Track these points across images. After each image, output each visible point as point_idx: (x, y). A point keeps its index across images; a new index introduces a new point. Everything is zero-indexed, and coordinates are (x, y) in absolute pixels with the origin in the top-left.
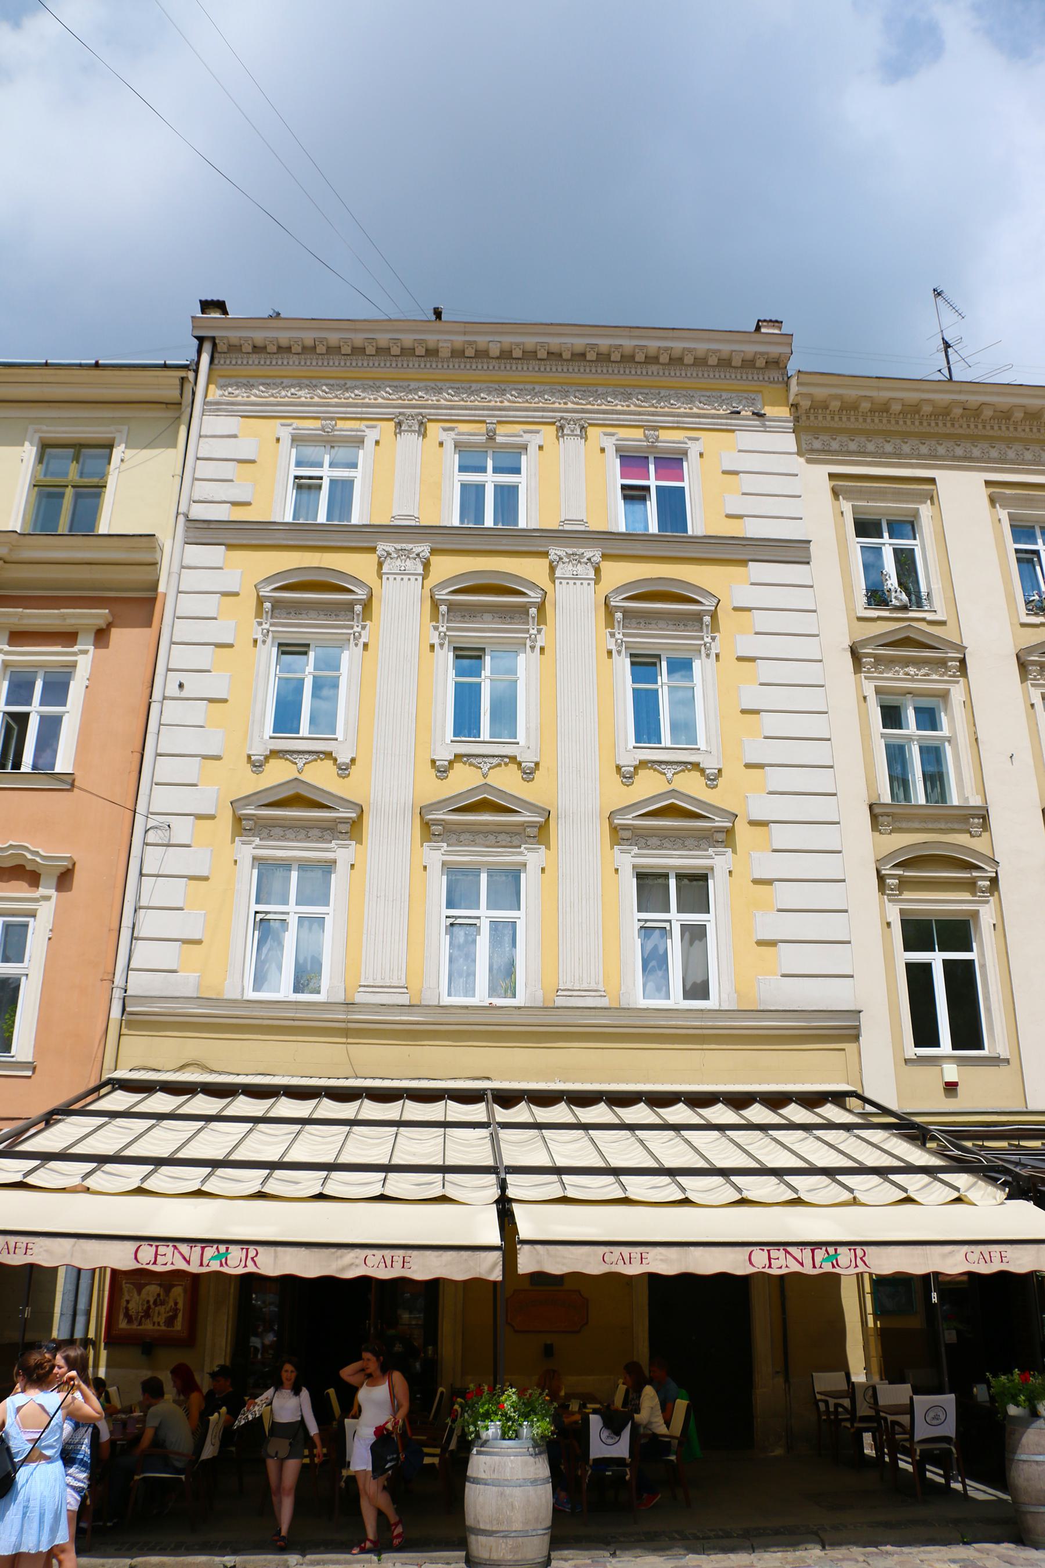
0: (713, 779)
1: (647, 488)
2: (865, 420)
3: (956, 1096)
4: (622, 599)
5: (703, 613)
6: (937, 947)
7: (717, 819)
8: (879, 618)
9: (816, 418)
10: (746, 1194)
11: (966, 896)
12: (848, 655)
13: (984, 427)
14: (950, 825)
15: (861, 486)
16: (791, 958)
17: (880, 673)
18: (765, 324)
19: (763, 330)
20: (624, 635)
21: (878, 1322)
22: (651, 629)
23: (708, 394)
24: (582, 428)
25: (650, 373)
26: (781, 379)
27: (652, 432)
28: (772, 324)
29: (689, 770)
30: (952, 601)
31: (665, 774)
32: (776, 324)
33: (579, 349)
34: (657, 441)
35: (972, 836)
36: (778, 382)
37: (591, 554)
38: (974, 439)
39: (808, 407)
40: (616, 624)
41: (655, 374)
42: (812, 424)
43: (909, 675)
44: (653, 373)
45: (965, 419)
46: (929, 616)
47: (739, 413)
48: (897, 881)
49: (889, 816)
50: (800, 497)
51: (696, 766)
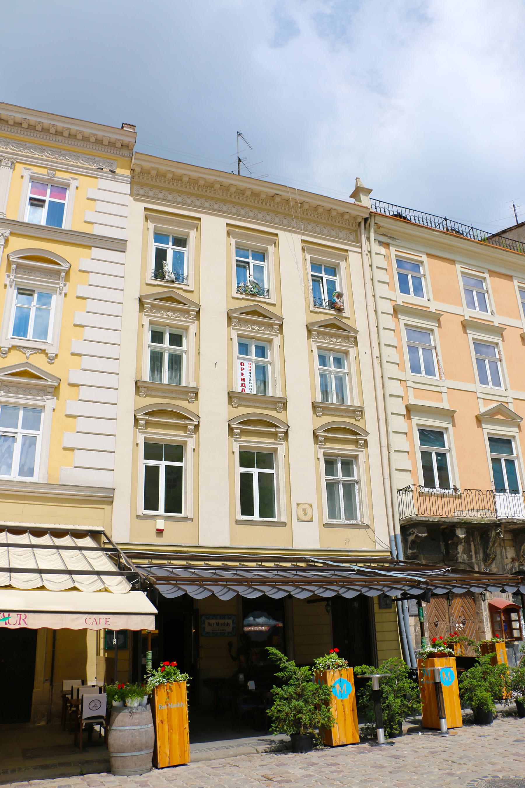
0: (52, 359)
1: (44, 201)
2: (169, 183)
3: (162, 537)
4: (17, 258)
5: (61, 271)
6: (163, 458)
7: (49, 380)
8: (158, 285)
9: (143, 178)
10: (77, 585)
11: (182, 433)
12: (137, 302)
13: (231, 196)
14: (178, 396)
15: (160, 217)
16: (80, 458)
17: (153, 313)
18: (126, 126)
19: (124, 129)
20: (15, 277)
21: (106, 653)
22: (31, 276)
23: (87, 157)
24: (13, 163)
25: (57, 140)
26: (128, 155)
27: (52, 172)
28: (130, 126)
29: (40, 353)
30: (198, 281)
31: (25, 354)
32: (132, 127)
33: (18, 120)
34: (54, 177)
35: (189, 402)
36: (127, 157)
37: (4, 231)
38: (225, 202)
39: (139, 172)
40: (12, 271)
41: (60, 141)
42: (141, 181)
43: (168, 316)
44: (59, 141)
45: (221, 191)
46: (185, 288)
47: (102, 169)
48: (145, 422)
49: (145, 388)
50: (127, 217)
51: (43, 351)
